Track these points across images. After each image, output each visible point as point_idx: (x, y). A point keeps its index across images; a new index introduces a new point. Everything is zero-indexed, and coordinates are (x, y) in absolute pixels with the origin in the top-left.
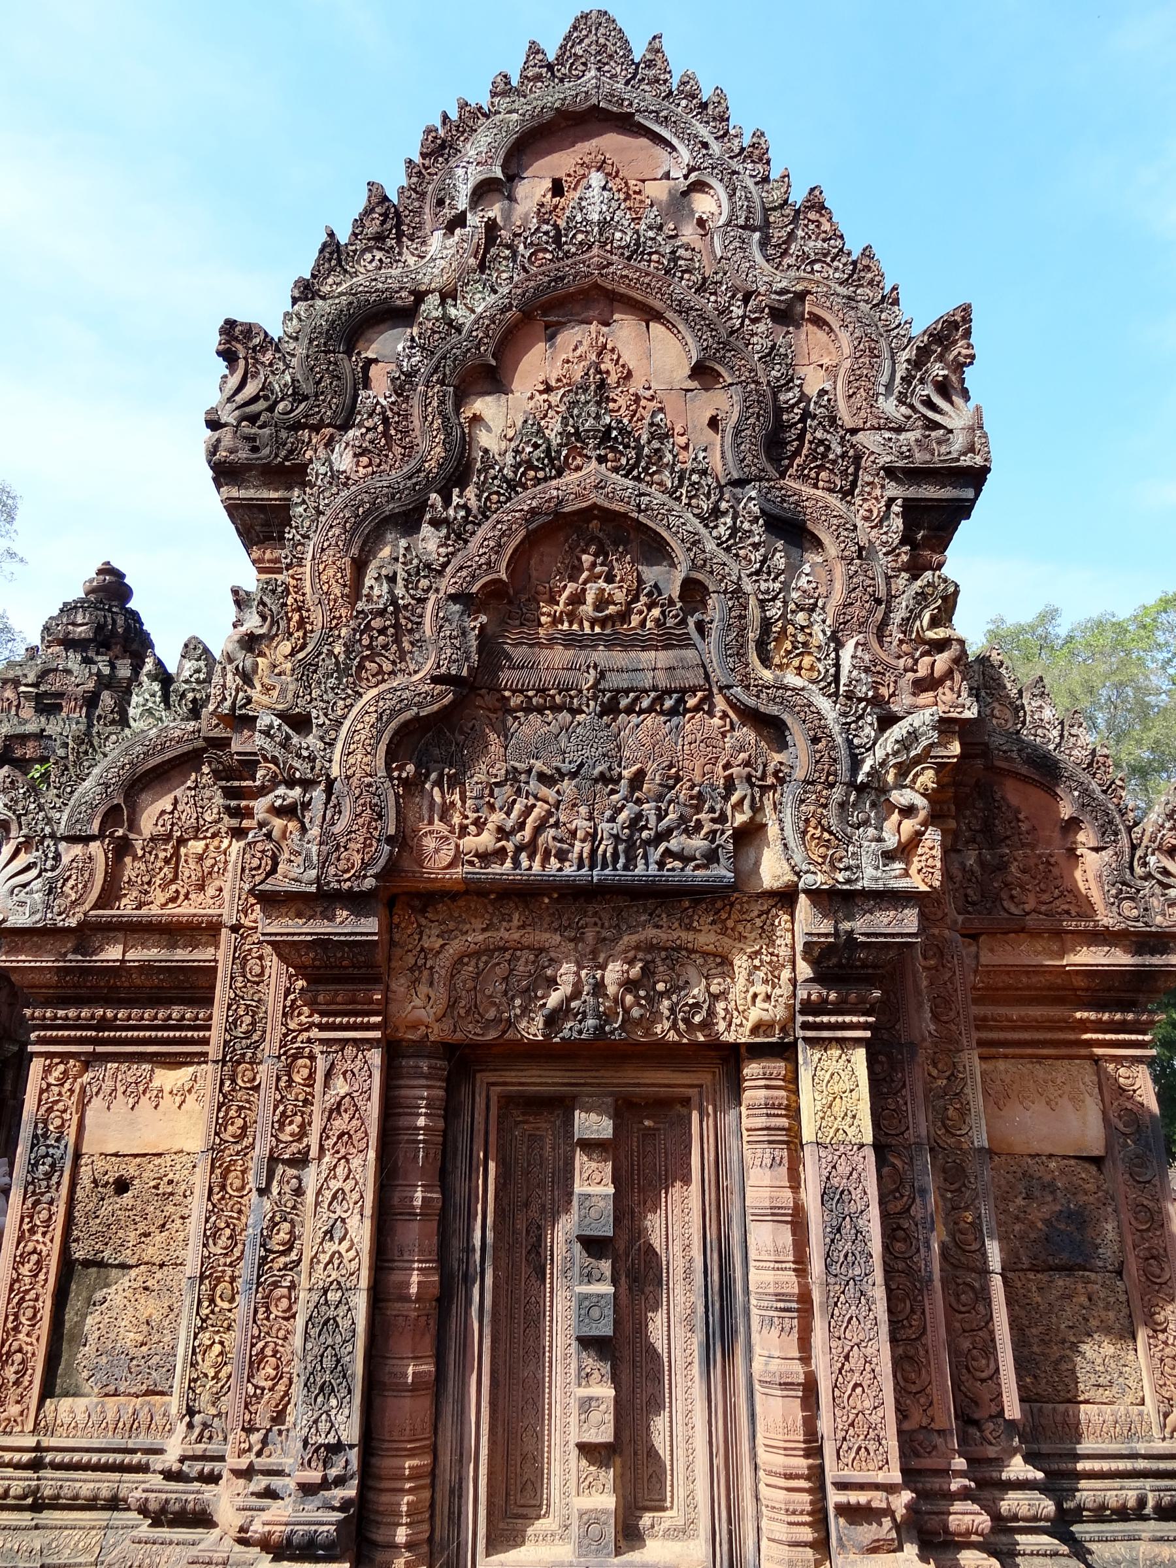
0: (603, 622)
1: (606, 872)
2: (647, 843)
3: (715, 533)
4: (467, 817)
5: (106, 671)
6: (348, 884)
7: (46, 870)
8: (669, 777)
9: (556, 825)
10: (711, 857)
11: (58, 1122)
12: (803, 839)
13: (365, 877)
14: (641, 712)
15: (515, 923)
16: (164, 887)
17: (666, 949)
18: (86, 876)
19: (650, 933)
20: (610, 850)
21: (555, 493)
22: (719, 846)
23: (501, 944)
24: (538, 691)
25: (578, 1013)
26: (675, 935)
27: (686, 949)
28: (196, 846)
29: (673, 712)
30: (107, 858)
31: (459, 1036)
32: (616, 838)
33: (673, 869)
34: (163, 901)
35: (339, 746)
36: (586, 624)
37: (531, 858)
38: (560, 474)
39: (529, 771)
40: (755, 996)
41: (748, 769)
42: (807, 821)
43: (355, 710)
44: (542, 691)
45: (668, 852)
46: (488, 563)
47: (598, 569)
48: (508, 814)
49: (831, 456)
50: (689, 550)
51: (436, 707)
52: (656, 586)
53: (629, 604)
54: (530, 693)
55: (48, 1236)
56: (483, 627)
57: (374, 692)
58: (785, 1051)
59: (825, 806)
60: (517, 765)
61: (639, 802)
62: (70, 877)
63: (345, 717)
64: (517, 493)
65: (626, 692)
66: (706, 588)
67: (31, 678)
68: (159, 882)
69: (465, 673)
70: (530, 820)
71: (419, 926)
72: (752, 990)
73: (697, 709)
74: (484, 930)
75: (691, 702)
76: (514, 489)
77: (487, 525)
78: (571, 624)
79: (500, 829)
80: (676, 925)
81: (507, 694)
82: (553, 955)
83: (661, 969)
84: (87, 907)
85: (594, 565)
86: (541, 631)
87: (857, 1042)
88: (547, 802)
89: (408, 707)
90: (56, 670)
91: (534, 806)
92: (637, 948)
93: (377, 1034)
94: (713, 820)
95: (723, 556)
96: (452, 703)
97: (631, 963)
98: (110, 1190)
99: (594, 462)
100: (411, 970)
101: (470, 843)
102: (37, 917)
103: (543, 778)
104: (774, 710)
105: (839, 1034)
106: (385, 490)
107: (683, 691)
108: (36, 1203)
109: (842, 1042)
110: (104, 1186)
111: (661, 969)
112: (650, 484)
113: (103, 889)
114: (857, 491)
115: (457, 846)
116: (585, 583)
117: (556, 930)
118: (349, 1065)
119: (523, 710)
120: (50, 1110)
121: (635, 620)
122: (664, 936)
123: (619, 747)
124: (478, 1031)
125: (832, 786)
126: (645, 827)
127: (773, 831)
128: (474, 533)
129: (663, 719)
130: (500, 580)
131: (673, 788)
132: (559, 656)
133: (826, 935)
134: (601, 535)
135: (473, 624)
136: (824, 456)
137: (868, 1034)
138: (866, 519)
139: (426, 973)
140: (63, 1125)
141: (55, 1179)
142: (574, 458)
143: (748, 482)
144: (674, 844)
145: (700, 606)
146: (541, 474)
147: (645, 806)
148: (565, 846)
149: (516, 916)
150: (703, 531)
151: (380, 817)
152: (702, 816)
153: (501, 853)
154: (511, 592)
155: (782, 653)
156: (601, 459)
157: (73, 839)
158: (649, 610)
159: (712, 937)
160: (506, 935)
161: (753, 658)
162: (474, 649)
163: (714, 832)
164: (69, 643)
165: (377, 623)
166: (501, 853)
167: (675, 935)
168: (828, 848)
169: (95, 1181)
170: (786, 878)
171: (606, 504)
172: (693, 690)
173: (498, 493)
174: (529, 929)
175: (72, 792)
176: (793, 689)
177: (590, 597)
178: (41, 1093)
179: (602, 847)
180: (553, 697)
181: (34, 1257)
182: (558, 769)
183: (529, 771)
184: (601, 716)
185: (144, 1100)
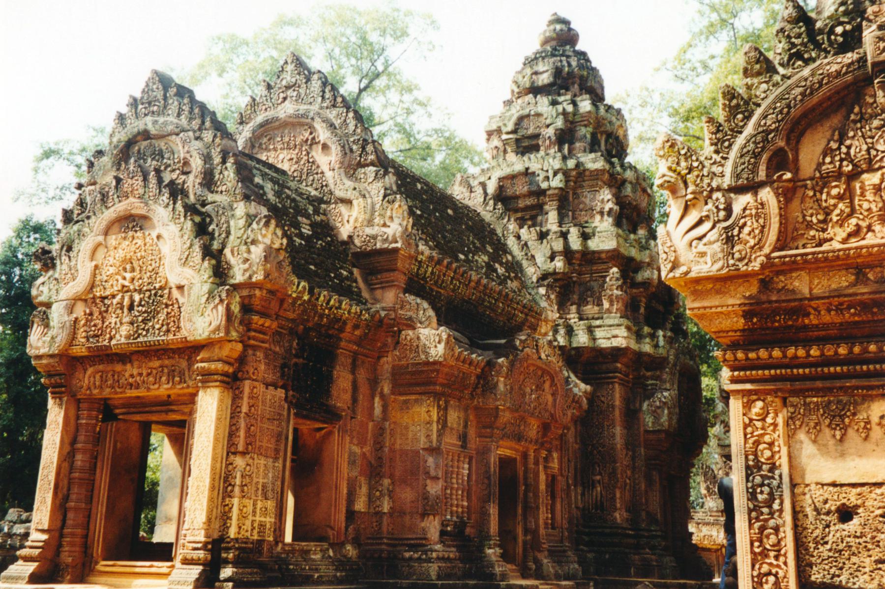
5: (570, 108)
7: (719, 221)
11: (768, 453)
16: (841, 223)
18: (761, 221)
28: (871, 179)
30: (779, 201)
34: (844, 235)
55: (782, 559)
62: (745, 224)
67: (510, 127)
68: (835, 219)
84: (767, 250)
90: (528, 116)
98: (833, 518)
102: (720, 264)
108: (762, 529)
110: (828, 513)
113: (780, 232)
120: (757, 443)
140: (773, 456)
141: (776, 506)
157: (739, 190)
164: (535, 90)
169: (816, 509)
175: (730, 145)
178: (745, 428)
181: (772, 579)
185: (851, 432)
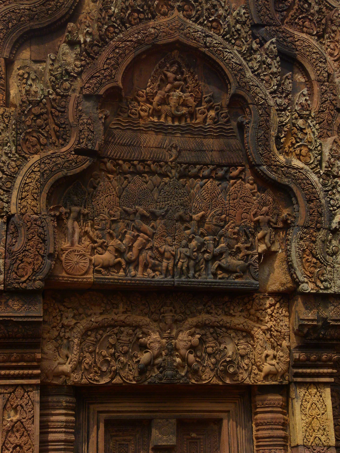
1: (183, 278)
2: (207, 261)
4: (96, 242)
6: (25, 284)
8: (221, 220)
9: (151, 248)
10: (245, 270)
12: (302, 262)
13: (35, 280)
14: (204, 178)
15: (121, 309)
17: (213, 327)
19: (204, 317)
20: (185, 265)
21: (153, 31)
22: (250, 264)
23: (112, 322)
24: (140, 161)
25: (160, 367)
26: (220, 318)
27: (226, 327)
29: (223, 179)
31: (84, 381)
32: (189, 258)
33: (222, 278)
35: (15, 193)
36: (169, 119)
37: (136, 268)
38: (154, 17)
39: (135, 213)
40: (267, 356)
41: (268, 217)
42: (304, 251)
43: (25, 169)
44: (142, 161)
45: (220, 267)
46: (110, 76)
48: (121, 240)
49: (312, 11)
51: (78, 170)
54: (136, 162)
57: (37, 157)
58: (283, 390)
59: (314, 242)
60: (128, 209)
61: (202, 235)
63: (16, 173)
64: (126, 28)
65: (195, 164)
66: (246, 101)
69: (96, 148)
70: (135, 244)
71: (60, 311)
72: (266, 352)
73: (237, 177)
74: (101, 314)
75: (235, 173)
76: (123, 23)
79: (117, 250)
80: (220, 311)
81: (121, 162)
82: (144, 330)
83: (210, 339)
86: (141, 122)
87: (326, 384)
88: (146, 234)
89: (60, 170)
91: (138, 236)
92: (197, 326)
93: (37, 381)
94: (247, 248)
95: (256, 81)
96: (89, 167)
97: (192, 335)
99: (176, 12)
100: (56, 339)
101: (97, 258)
103: (143, 217)
104: (285, 181)
105: (316, 380)
106: (27, 12)
107: (229, 165)
109: (317, 385)
111: (210, 339)
114: (327, 36)
115: (91, 260)
117: (146, 314)
118: (19, 402)
119: (130, 173)
121: (201, 118)
122: (213, 319)
123: (190, 199)
124: (97, 378)
125: (318, 230)
126: (206, 252)
127: (281, 254)
129: (217, 182)
130: (118, 87)
131: (223, 227)
132: (152, 140)
133: (312, 320)
134: (179, 60)
135: (100, 115)
136: (307, 11)
137: (332, 380)
138: (331, 55)
139: (65, 341)
142: (162, 6)
143: (263, 26)
144: (223, 262)
146: (142, 16)
147: (206, 238)
148: (157, 262)
149: (121, 305)
150: (244, 63)
151: (44, 241)
152: (239, 245)
153: (118, 265)
155: (289, 144)
156: (180, 9)
158: (208, 111)
159: (242, 320)
160: (116, 317)
161: (274, 147)
163: (248, 255)
165: (36, 110)
166: (118, 265)
167: (220, 318)
168: (316, 268)
170: (289, 285)
171: (185, 41)
172: (236, 166)
174: (129, 314)
176: (297, 169)
177: (173, 101)
179: (180, 264)
180: (149, 166)
182: (153, 213)
183: (135, 213)
184: (179, 179)
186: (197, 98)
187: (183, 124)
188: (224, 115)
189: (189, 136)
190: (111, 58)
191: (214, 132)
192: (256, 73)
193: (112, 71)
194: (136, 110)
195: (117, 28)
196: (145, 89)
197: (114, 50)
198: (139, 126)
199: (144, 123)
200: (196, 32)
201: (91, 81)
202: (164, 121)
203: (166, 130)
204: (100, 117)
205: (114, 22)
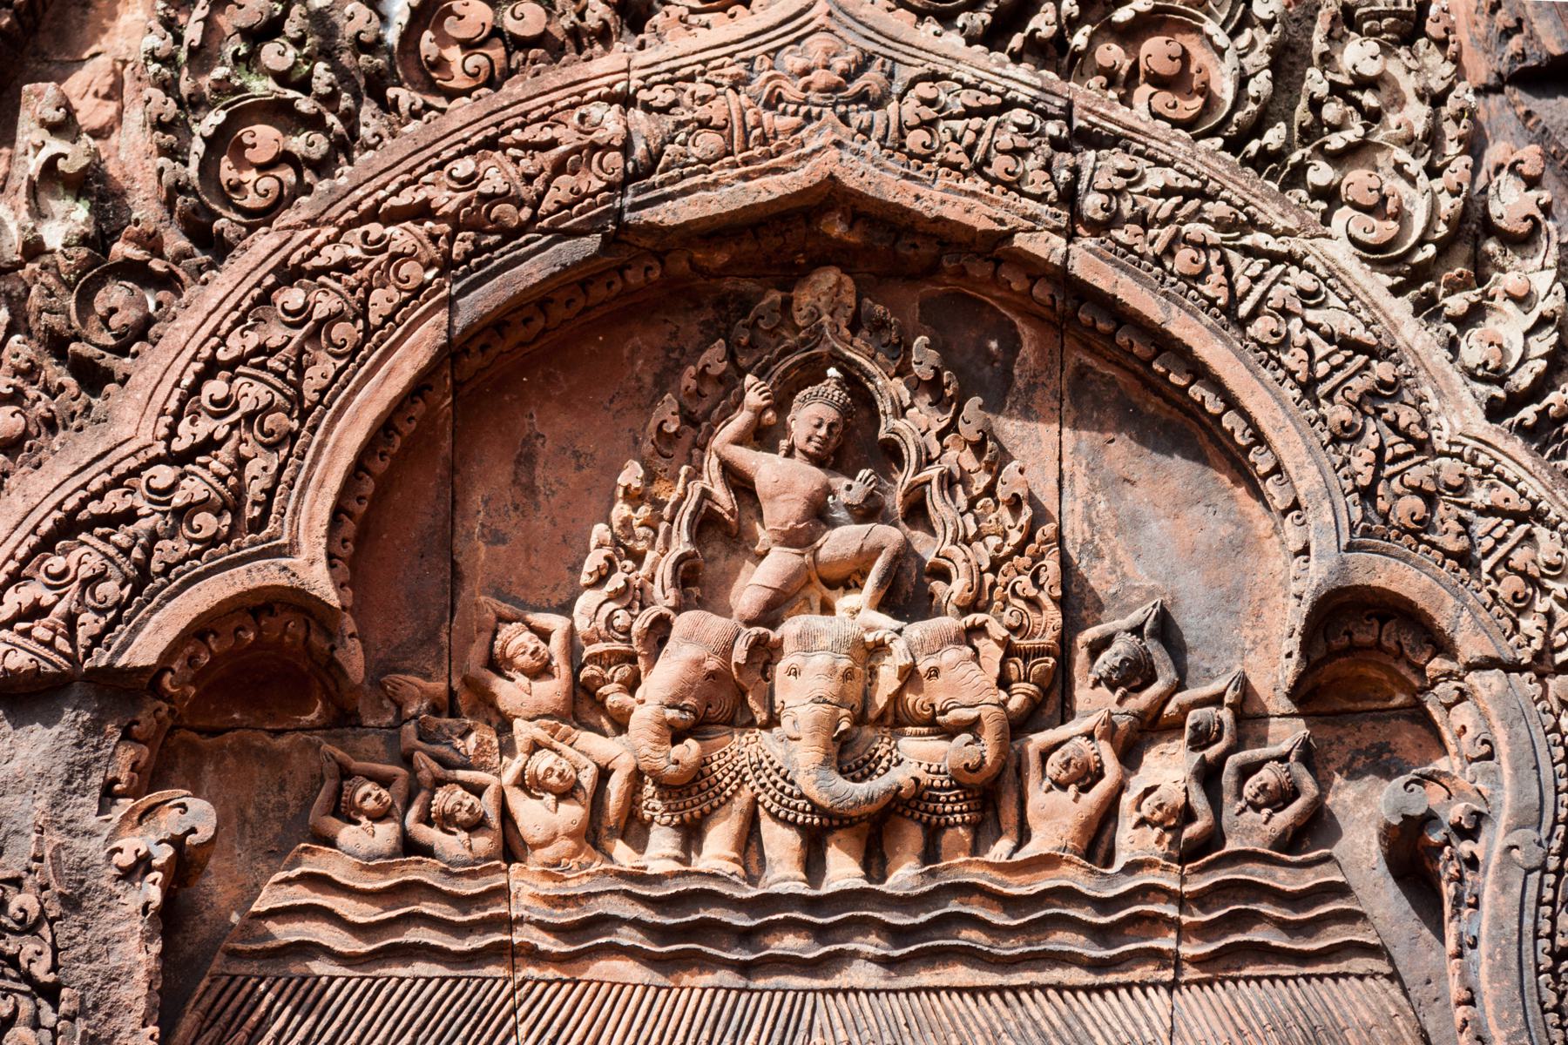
0: (875, 832)
3: (1474, 350)
36: (780, 843)
47: (841, 541)
50: (1346, 435)
52: (1165, 628)
53: (1019, 726)
56: (186, 864)
77: (227, 284)
78: (692, 834)
85: (819, 513)
112: (1123, 83)
116: (773, 611)
121: (1054, 817)
128: (142, 330)
130: (296, 601)
135: (132, 844)
145: (1406, 738)
150: (1414, 335)
154: (354, 659)
158: (1130, 756)
162: (135, 993)
173: (280, 113)
186: (1026, 655)
187: (904, 875)
188: (1267, 775)
189: (961, 974)
190: (241, 360)
191: (1183, 932)
192: (1529, 414)
193: (241, 461)
194: (477, 790)
195: (314, 123)
196: (566, 609)
197: (265, 299)
198: (508, 923)
199: (549, 888)
200: (985, 112)
201: (56, 563)
202: (728, 868)
203: (745, 937)
204: (126, 859)
205: (282, 78)
